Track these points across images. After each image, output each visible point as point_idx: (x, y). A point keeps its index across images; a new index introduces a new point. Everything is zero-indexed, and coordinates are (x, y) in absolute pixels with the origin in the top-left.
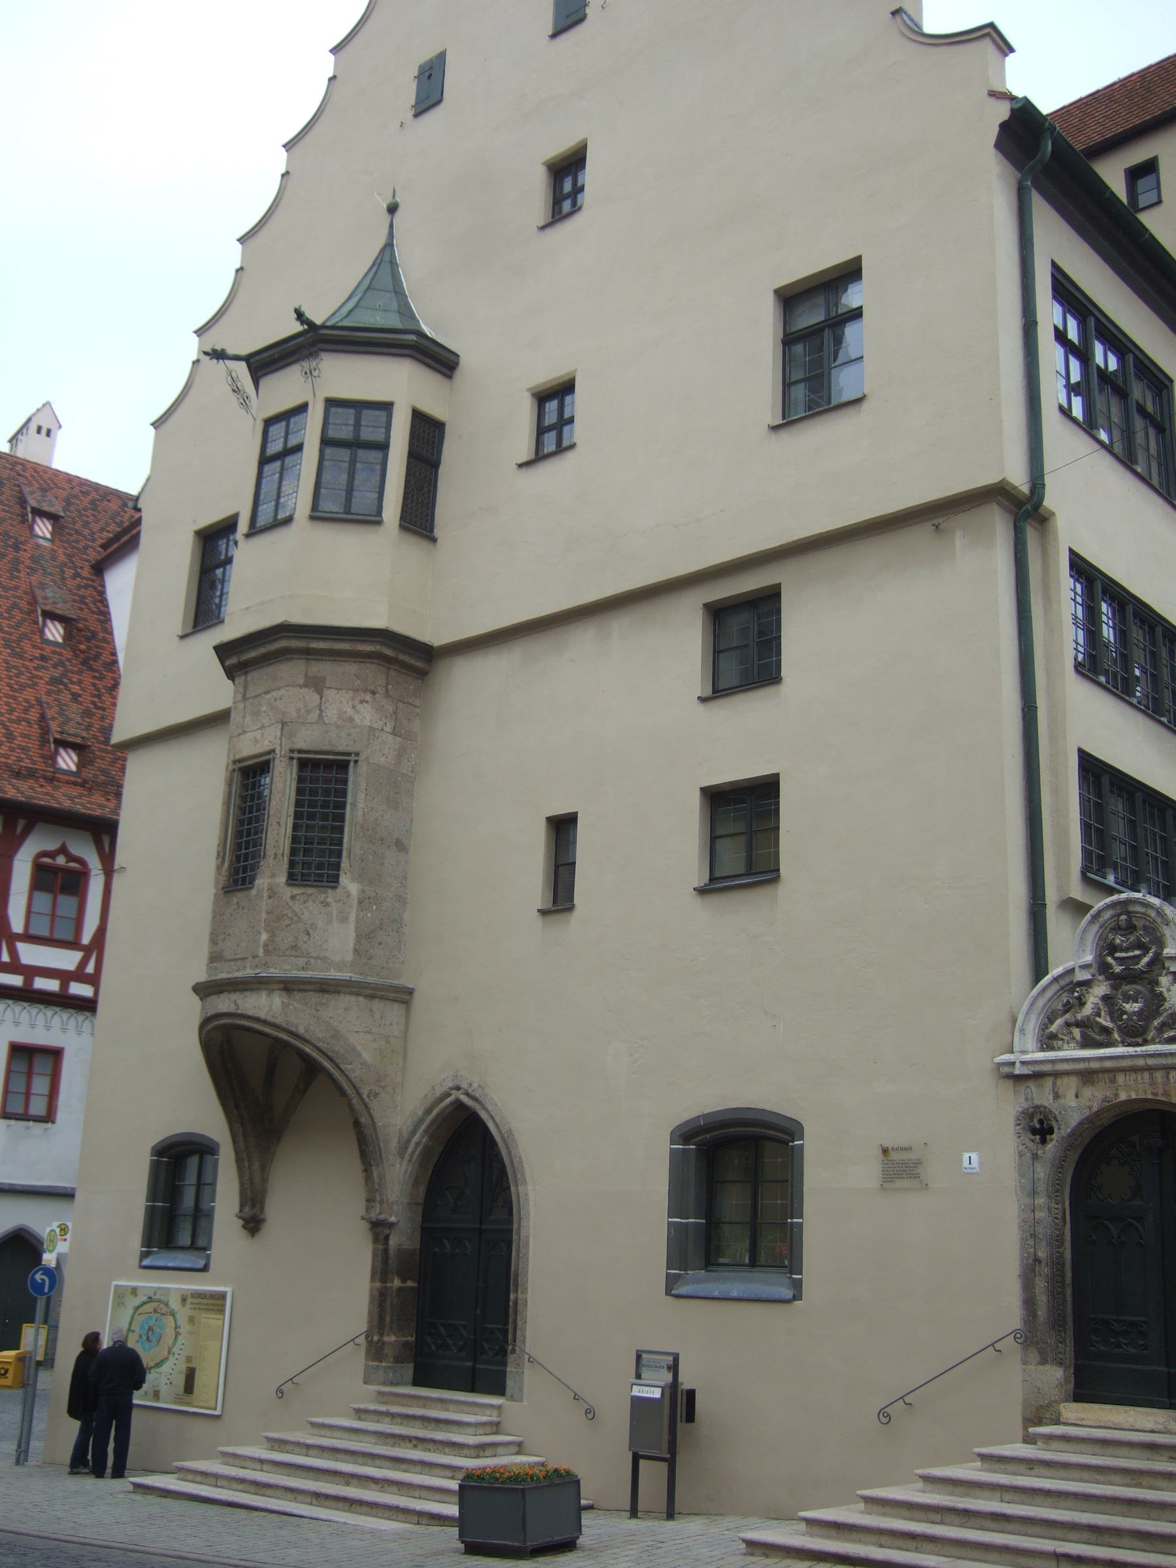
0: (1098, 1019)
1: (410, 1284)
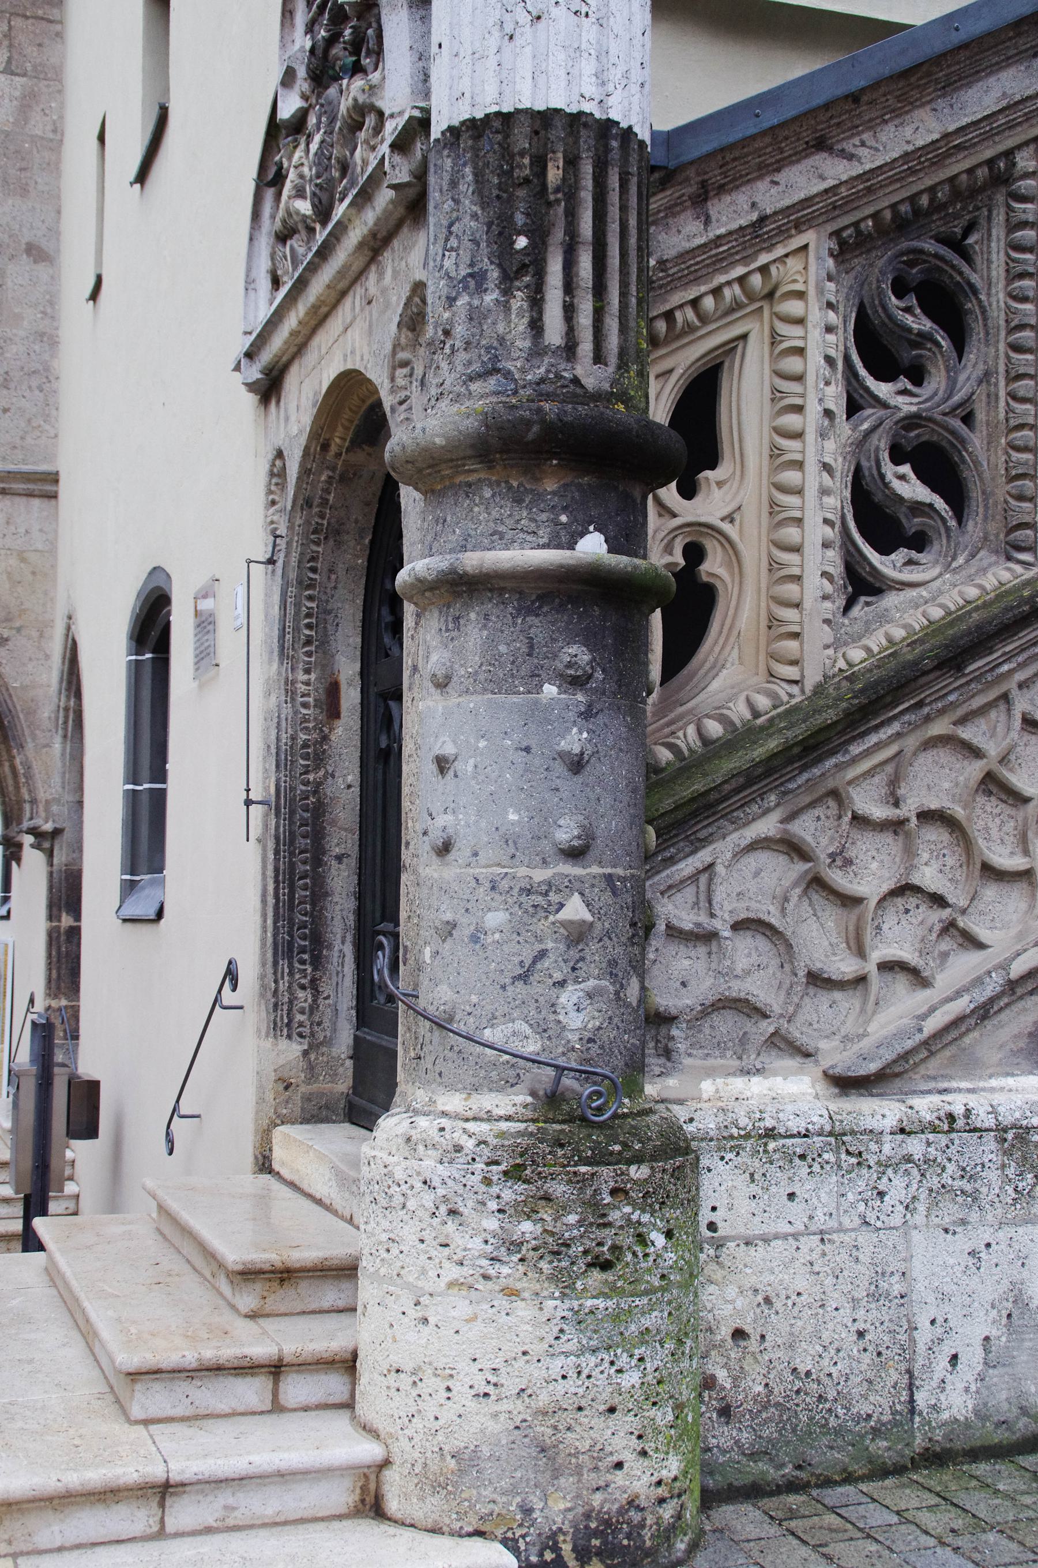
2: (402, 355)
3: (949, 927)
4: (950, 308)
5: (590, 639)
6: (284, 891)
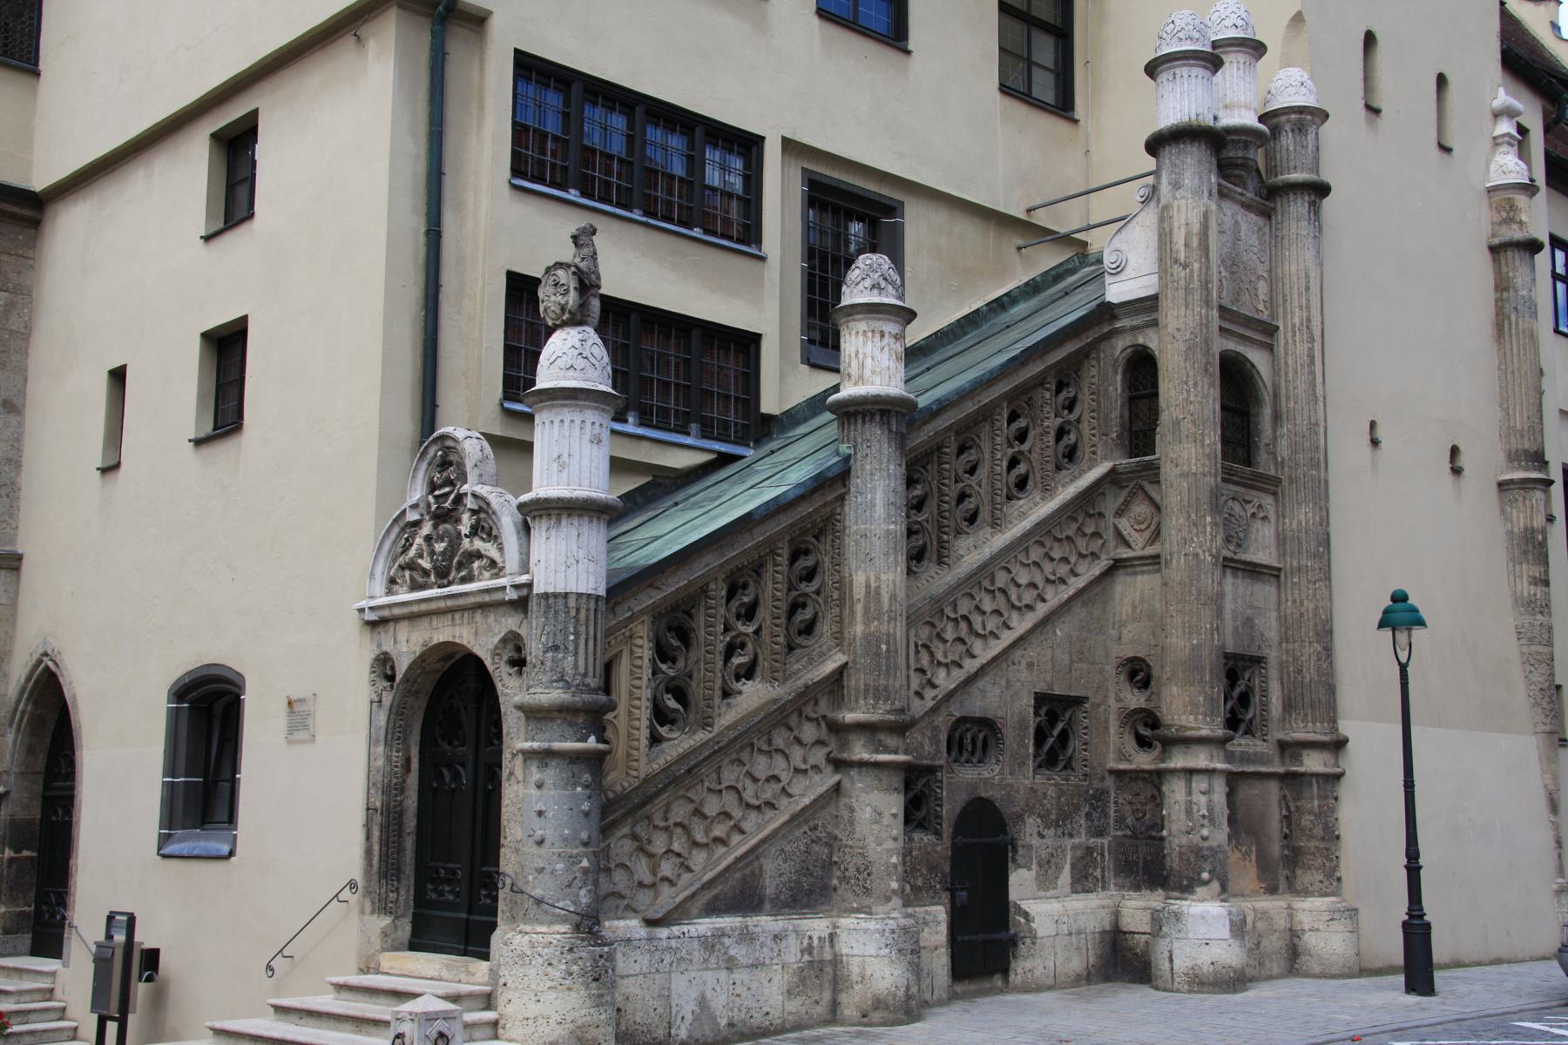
1: (26, 853)
3: (682, 864)
4: (685, 636)
5: (592, 774)
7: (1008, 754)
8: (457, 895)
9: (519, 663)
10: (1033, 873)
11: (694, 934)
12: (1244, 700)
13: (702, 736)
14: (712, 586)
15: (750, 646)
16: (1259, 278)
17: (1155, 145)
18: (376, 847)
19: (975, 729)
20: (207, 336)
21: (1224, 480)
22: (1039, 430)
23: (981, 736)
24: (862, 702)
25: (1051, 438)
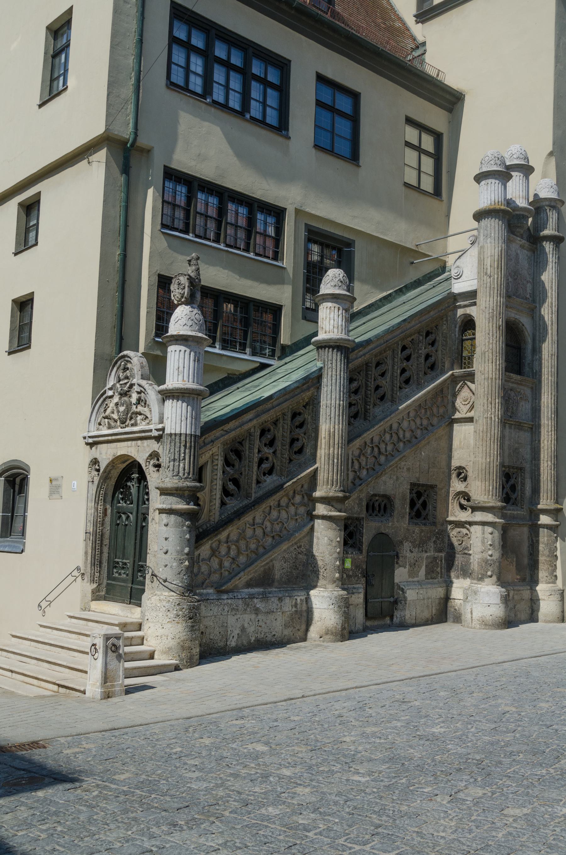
0: (112, 415)
2: (148, 460)
4: (238, 454)
6: (94, 552)
7: (396, 512)
8: (127, 575)
9: (158, 466)
10: (407, 570)
11: (240, 597)
12: (513, 488)
13: (246, 502)
14: (252, 430)
15: (271, 459)
16: (528, 282)
17: (479, 216)
18: (90, 551)
19: (381, 499)
20: (14, 301)
21: (506, 381)
22: (416, 355)
23: (383, 504)
24: (325, 487)
25: (422, 360)
